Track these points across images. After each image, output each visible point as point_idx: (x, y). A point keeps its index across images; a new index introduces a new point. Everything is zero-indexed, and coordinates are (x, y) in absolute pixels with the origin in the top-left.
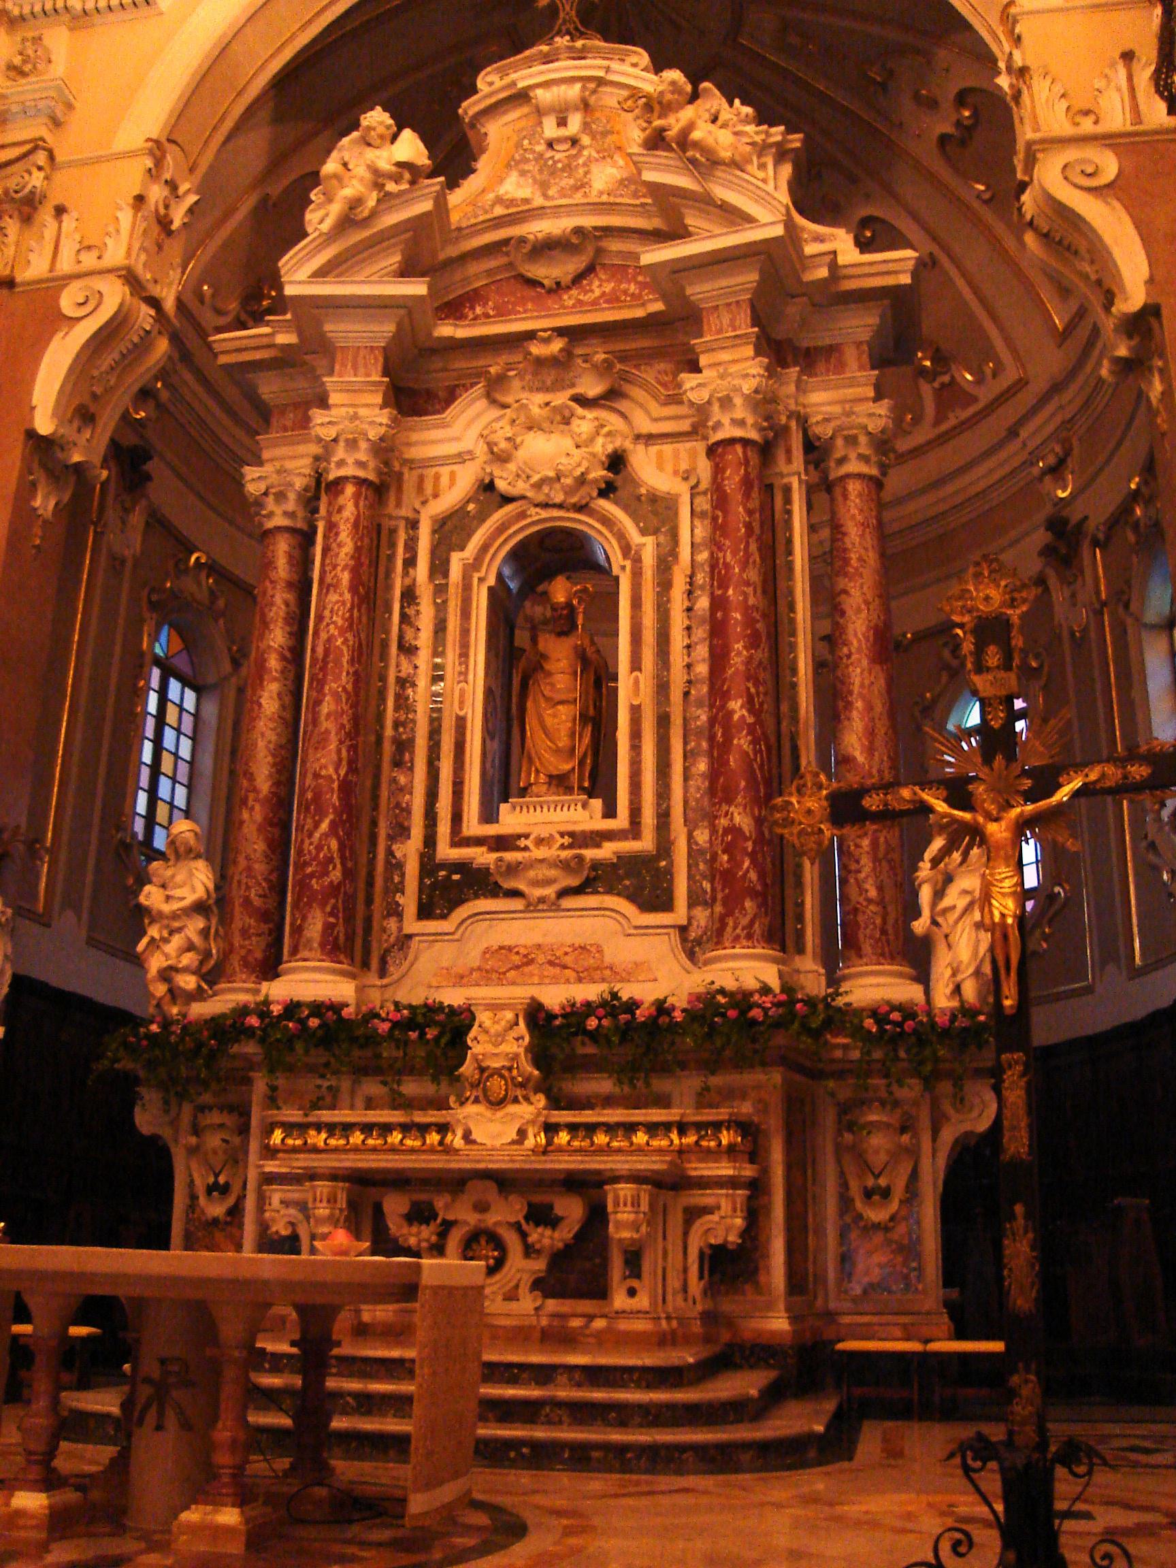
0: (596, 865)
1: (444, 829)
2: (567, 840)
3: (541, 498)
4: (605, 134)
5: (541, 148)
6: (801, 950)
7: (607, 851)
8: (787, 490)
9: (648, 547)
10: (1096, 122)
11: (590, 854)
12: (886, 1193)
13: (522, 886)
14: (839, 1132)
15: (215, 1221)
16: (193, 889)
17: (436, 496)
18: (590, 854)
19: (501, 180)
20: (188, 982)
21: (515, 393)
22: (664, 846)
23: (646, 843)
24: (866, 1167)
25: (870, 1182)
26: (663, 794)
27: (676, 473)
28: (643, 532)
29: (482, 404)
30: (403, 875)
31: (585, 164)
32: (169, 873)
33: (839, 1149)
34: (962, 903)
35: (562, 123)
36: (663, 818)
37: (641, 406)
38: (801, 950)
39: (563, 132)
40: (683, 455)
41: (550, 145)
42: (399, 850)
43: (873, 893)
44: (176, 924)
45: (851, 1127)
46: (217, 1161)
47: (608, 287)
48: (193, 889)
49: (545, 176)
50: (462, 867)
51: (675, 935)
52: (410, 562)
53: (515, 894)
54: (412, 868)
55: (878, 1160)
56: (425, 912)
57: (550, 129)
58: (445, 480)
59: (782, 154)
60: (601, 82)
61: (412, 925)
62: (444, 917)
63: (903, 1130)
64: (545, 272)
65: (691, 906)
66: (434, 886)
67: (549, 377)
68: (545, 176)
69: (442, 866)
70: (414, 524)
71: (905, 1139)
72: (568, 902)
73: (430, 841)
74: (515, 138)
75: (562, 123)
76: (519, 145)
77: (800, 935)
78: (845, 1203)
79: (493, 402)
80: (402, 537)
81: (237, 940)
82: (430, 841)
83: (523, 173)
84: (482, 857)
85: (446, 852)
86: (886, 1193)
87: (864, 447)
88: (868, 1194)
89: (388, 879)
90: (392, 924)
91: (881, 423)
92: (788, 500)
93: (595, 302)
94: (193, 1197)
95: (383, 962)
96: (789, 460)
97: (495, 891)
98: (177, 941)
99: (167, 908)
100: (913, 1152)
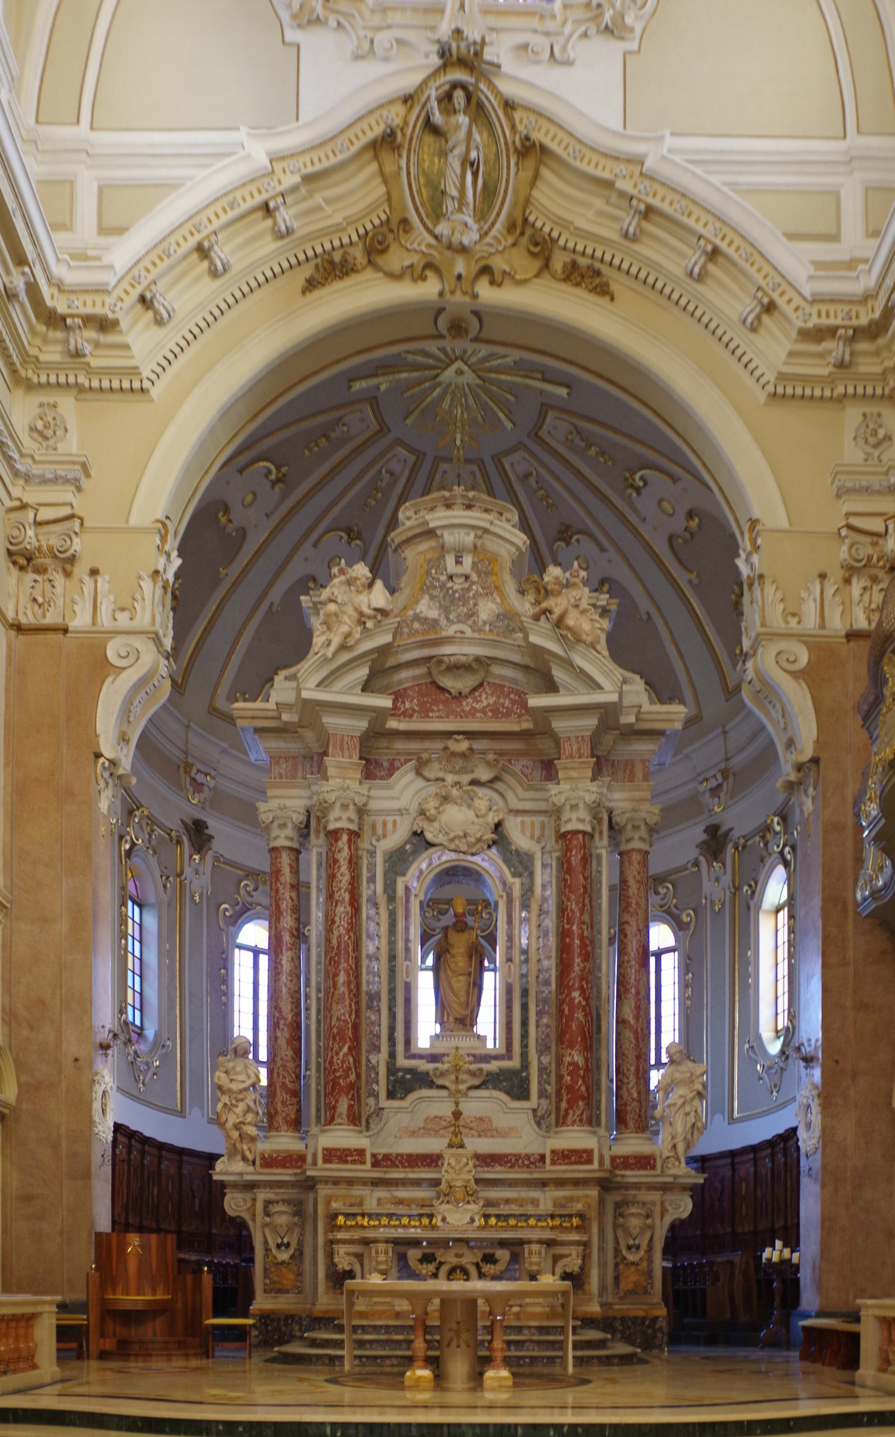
0: (489, 1074)
1: (400, 1048)
2: (471, 1058)
3: (453, 847)
4: (488, 574)
5: (443, 578)
6: (599, 1124)
7: (494, 1066)
8: (599, 858)
9: (516, 884)
10: (799, 622)
11: (485, 1067)
12: (638, 1247)
13: (447, 1084)
14: (615, 1217)
15: (283, 1262)
16: (249, 1077)
17: (385, 836)
18: (485, 1067)
19: (417, 602)
20: (252, 1131)
21: (433, 771)
22: (525, 1066)
23: (515, 1063)
24: (628, 1233)
25: (631, 1242)
26: (525, 1036)
27: (532, 837)
28: (514, 875)
29: (411, 776)
30: (377, 1074)
31: (474, 597)
32: (231, 1065)
33: (616, 1226)
34: (680, 1102)
35: (458, 562)
36: (525, 1046)
37: (513, 790)
38: (599, 1124)
39: (459, 570)
40: (537, 825)
41: (451, 577)
42: (373, 1059)
43: (635, 1095)
44: (241, 1096)
45: (622, 1215)
46: (282, 1231)
47: (492, 700)
48: (249, 1077)
49: (447, 603)
50: (411, 1071)
51: (530, 1113)
52: (372, 879)
53: (443, 1087)
54: (382, 1070)
55: (635, 1232)
56: (391, 1095)
57: (450, 560)
58: (390, 826)
59: (604, 612)
60: (486, 531)
61: (384, 1102)
62: (402, 1098)
63: (648, 1216)
64: (447, 682)
65: (539, 1098)
66: (395, 1081)
67: (459, 763)
68: (447, 603)
69: (399, 1070)
70: (372, 854)
71: (649, 1221)
72: (473, 1093)
73: (392, 1055)
74: (425, 567)
75: (458, 562)
76: (428, 573)
77: (599, 1117)
78: (617, 1251)
79: (419, 773)
80: (365, 862)
81: (279, 1107)
82: (392, 1055)
83: (432, 598)
84: (424, 1066)
85: (402, 1062)
86: (638, 1247)
87: (643, 832)
88: (629, 1248)
89: (368, 1076)
90: (371, 1101)
91: (655, 819)
92: (599, 864)
93: (483, 711)
94: (267, 1250)
95: (368, 1122)
96: (601, 839)
97: (431, 1085)
98: (241, 1106)
99: (234, 1087)
100: (651, 1227)
